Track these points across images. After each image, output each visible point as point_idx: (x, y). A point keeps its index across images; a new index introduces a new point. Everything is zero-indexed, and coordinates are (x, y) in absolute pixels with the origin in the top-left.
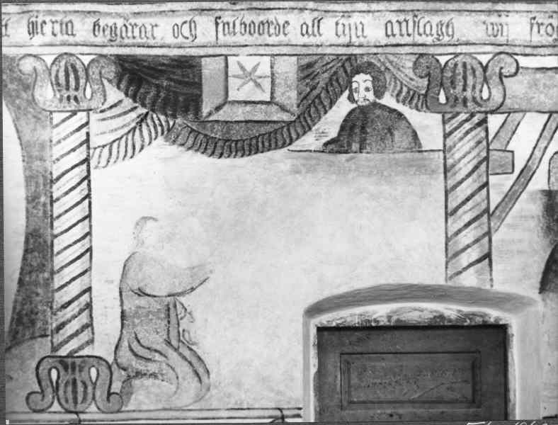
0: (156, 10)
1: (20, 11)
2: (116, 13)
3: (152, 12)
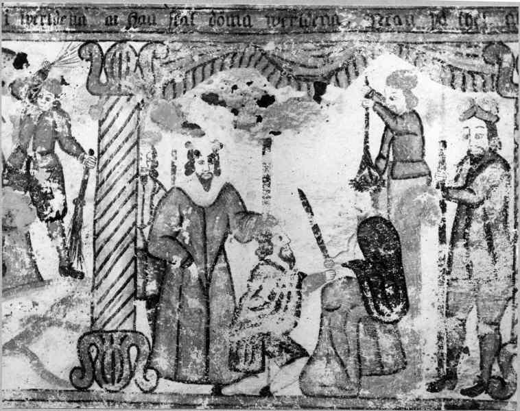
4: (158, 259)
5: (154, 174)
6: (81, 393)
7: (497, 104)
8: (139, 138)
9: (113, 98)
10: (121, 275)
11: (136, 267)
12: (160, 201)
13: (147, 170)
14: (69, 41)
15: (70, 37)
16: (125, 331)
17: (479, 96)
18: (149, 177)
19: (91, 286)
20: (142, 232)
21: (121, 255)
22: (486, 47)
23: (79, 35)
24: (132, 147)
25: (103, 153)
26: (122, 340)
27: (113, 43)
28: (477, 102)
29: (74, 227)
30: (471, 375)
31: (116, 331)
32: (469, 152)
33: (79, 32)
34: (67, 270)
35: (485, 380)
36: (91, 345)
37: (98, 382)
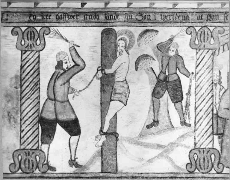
4: (222, 118)
5: (220, 82)
6: (191, 174)
8: (213, 67)
9: (202, 51)
10: (207, 125)
11: (213, 121)
12: (223, 94)
13: (217, 81)
14: (182, 26)
15: (182, 25)
16: (209, 148)
18: (218, 84)
19: (194, 129)
20: (215, 107)
21: (207, 116)
23: (187, 24)
24: (210, 71)
25: (198, 73)
26: (208, 152)
27: (201, 27)
29: (186, 105)
31: (206, 148)
33: (186, 22)
34: (184, 123)
36: (195, 154)
37: (198, 169)
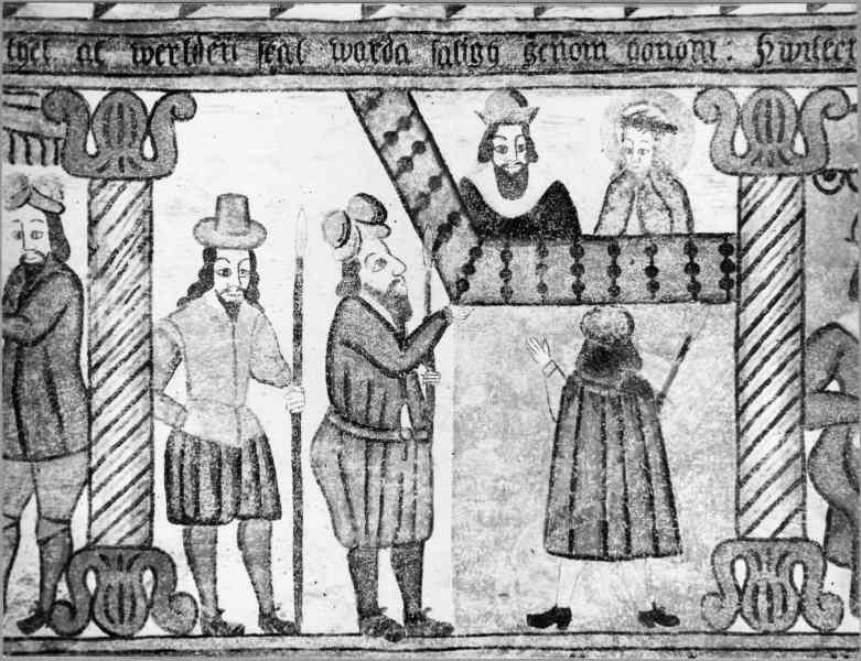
0: (267, 646)
1: (43, 649)
2: (201, 651)
3: (260, 649)
7: (62, 186)
17: (35, 172)
22: (47, 96)
28: (31, 181)
30: (24, 601)
32: (23, 258)
35: (46, 607)
